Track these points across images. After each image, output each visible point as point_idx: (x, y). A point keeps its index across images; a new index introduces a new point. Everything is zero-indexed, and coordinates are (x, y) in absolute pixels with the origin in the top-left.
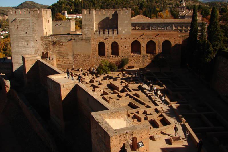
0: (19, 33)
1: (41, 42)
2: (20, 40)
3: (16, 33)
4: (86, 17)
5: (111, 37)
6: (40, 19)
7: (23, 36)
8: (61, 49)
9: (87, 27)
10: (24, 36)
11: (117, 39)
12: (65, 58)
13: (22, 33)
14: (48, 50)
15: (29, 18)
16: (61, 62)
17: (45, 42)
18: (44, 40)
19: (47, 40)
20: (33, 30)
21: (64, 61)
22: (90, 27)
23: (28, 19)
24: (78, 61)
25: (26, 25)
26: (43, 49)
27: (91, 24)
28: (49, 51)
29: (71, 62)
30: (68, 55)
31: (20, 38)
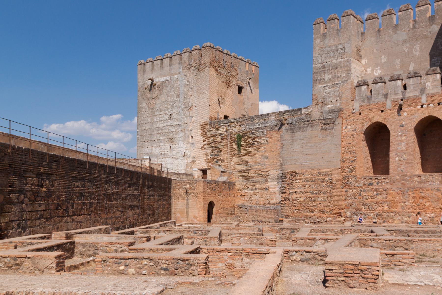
0: (155, 120)
1: (202, 138)
2: (155, 138)
3: (149, 120)
4: (327, 41)
5: (415, 100)
6: (202, 74)
7: (162, 125)
8: (251, 159)
9: (327, 77)
10: (165, 125)
11: (439, 104)
12: (258, 186)
13: (161, 119)
14: (217, 162)
15: (179, 73)
16: (246, 199)
17: (212, 139)
18: (209, 134)
19: (217, 132)
20: (186, 107)
21: (256, 197)
22: (339, 75)
23: (176, 76)
24: (295, 196)
25: (172, 96)
26: (205, 160)
27: (340, 62)
28: (220, 166)
29: (274, 201)
30: (267, 175)
31: (156, 132)
